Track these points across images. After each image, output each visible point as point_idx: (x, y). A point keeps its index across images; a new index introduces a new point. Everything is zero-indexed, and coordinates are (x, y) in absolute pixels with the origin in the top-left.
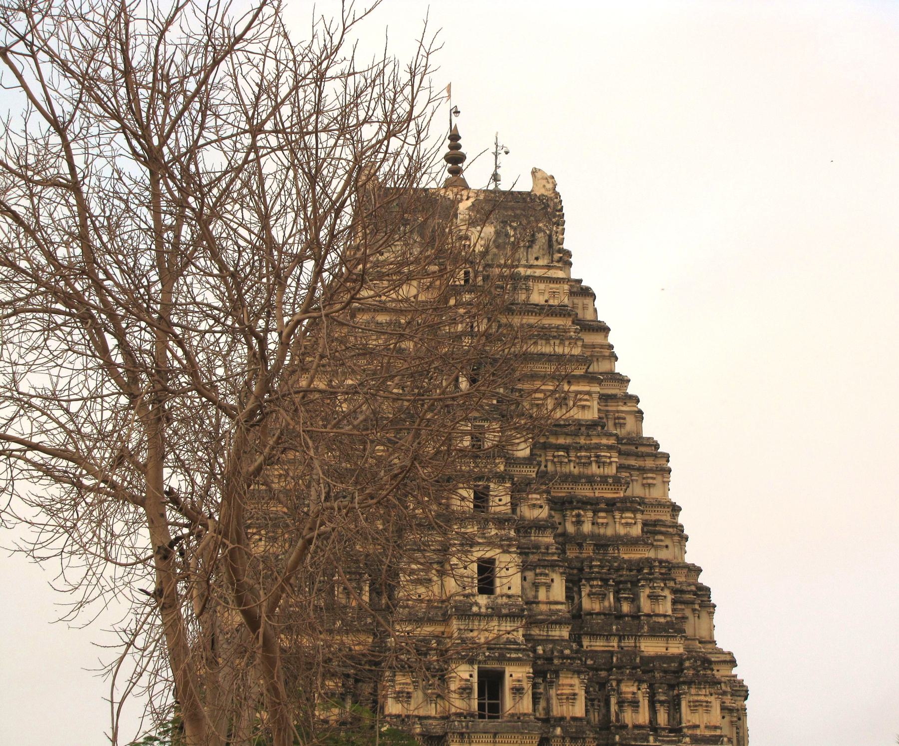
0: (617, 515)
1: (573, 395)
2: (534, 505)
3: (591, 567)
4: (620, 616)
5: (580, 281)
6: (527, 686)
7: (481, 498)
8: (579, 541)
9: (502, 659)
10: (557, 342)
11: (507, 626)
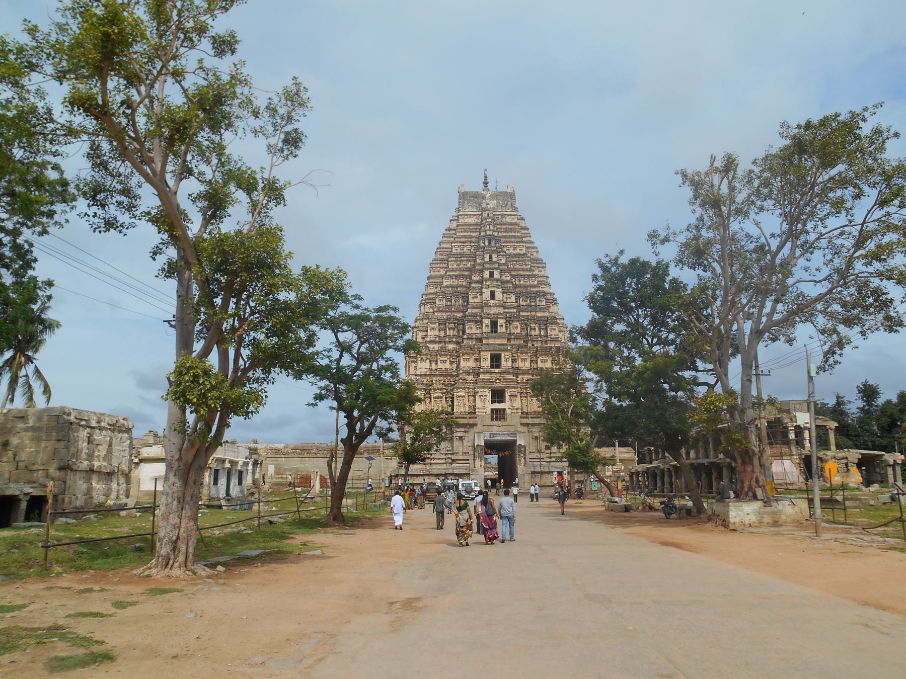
7: (492, 274)
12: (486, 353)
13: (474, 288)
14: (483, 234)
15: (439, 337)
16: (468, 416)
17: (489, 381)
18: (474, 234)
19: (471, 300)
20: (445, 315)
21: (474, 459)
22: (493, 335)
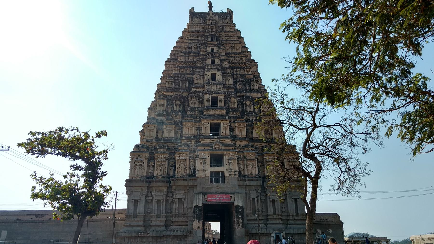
0: (245, 70)
3: (239, 79)
4: (246, 90)
6: (223, 100)
7: (213, 62)
8: (237, 75)
9: (217, 94)
13: (199, 72)
14: (206, 34)
15: (167, 112)
16: (187, 179)
17: (210, 145)
18: (199, 39)
19: (195, 81)
21: (193, 221)
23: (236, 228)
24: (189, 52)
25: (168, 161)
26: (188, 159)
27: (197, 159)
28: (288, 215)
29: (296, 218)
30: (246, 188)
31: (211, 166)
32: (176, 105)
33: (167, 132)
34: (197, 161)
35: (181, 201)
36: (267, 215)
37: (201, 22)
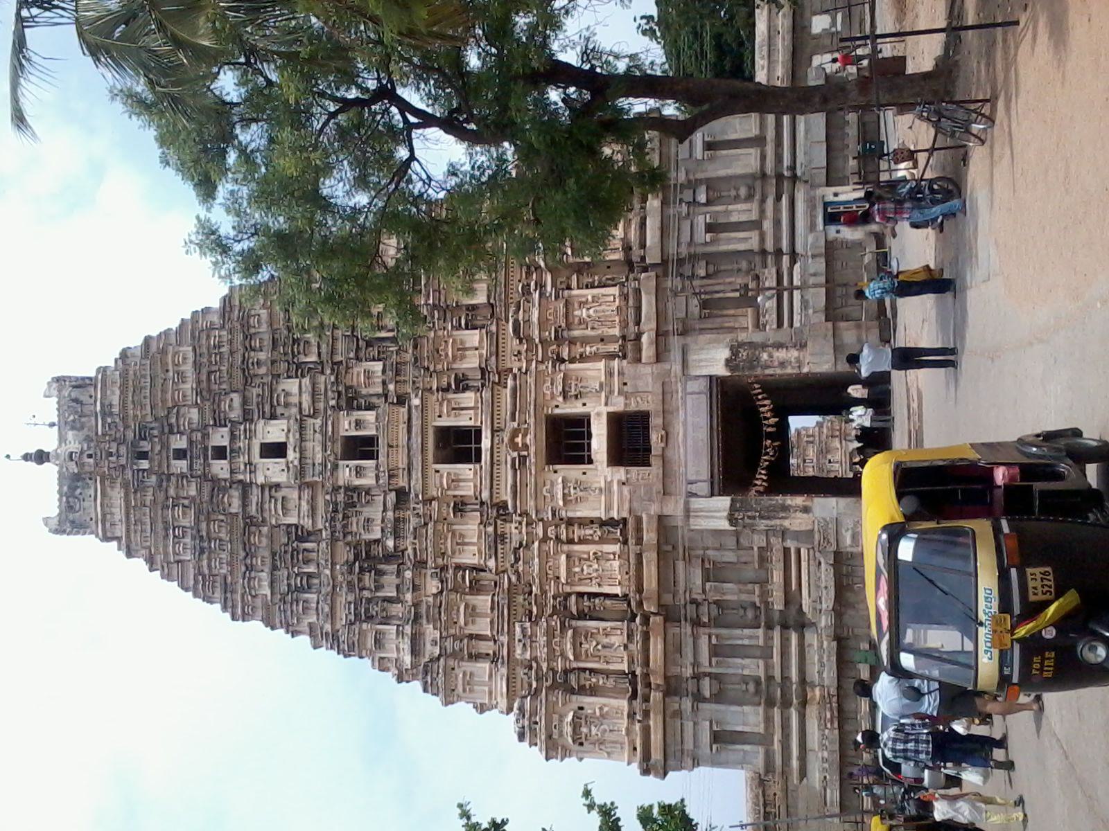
0: (252, 331)
1: (176, 368)
2: (230, 406)
5: (116, 361)
7: (220, 453)
10: (143, 380)
11: (310, 432)
12: (433, 479)
13: (261, 508)
16: (633, 547)
19: (292, 520)
20: (343, 597)
22: (383, 450)
23: (805, 370)
24: (193, 538)
25: (573, 617)
26: (565, 548)
27: (563, 514)
28: (764, 176)
29: (770, 149)
30: (666, 334)
31: (590, 462)
32: (379, 587)
33: (473, 622)
34: (571, 514)
35: (713, 573)
36: (763, 252)
37: (92, 492)
